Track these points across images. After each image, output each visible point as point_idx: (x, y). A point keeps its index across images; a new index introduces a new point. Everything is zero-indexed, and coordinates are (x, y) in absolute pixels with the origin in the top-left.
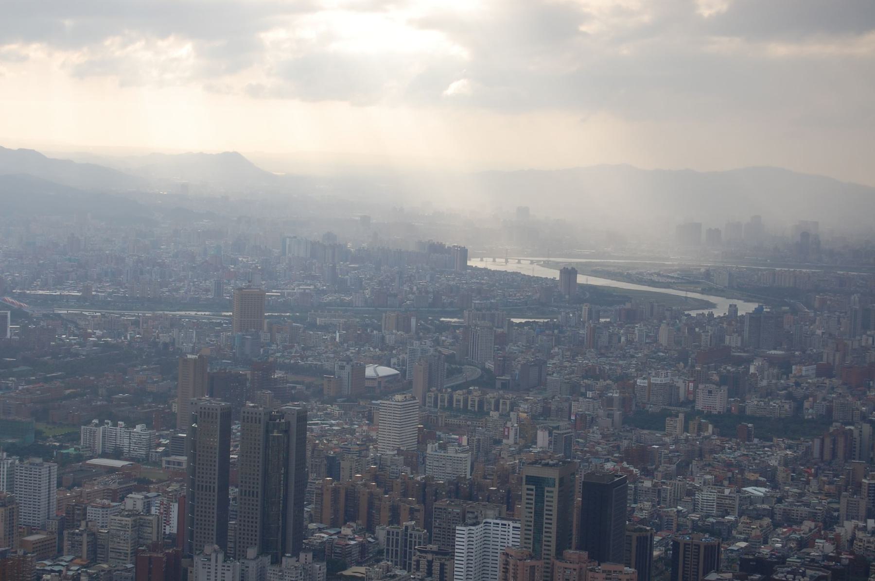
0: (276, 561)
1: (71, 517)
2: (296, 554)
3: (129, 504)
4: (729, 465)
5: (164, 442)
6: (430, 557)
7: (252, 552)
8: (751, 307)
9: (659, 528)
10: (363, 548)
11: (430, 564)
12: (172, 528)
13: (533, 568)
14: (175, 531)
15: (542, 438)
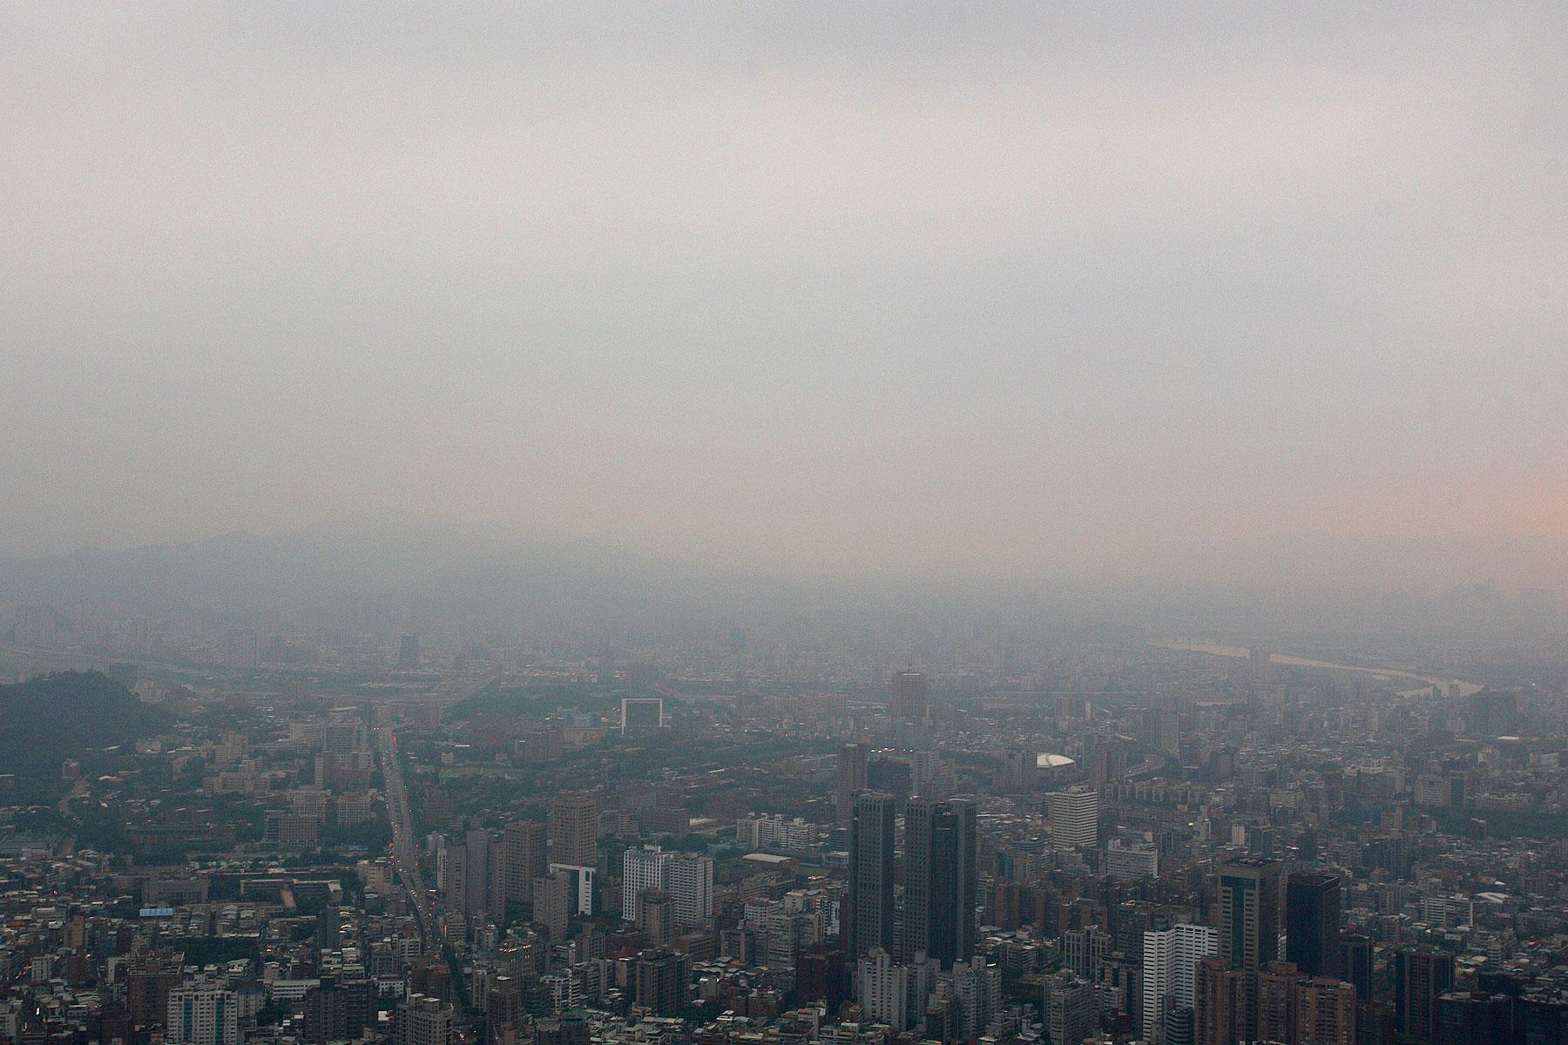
0: (946, 967)
1: (728, 916)
2: (967, 959)
3: (788, 901)
4: (1458, 867)
5: (823, 835)
6: (1115, 965)
7: (920, 956)
8: (1476, 689)
9: (1379, 938)
10: (1041, 953)
11: (1116, 973)
12: (835, 929)
13: (1233, 979)
14: (837, 931)
15: (1239, 835)
